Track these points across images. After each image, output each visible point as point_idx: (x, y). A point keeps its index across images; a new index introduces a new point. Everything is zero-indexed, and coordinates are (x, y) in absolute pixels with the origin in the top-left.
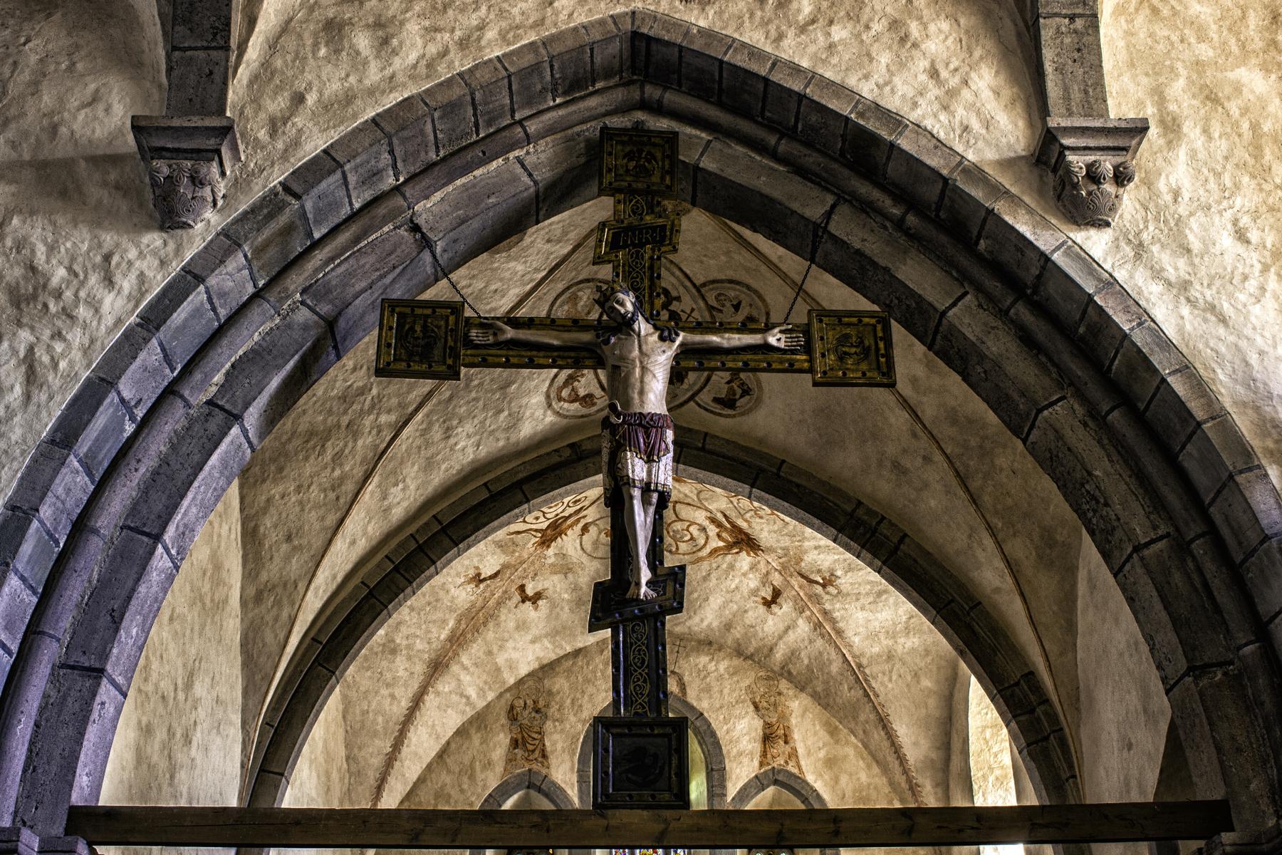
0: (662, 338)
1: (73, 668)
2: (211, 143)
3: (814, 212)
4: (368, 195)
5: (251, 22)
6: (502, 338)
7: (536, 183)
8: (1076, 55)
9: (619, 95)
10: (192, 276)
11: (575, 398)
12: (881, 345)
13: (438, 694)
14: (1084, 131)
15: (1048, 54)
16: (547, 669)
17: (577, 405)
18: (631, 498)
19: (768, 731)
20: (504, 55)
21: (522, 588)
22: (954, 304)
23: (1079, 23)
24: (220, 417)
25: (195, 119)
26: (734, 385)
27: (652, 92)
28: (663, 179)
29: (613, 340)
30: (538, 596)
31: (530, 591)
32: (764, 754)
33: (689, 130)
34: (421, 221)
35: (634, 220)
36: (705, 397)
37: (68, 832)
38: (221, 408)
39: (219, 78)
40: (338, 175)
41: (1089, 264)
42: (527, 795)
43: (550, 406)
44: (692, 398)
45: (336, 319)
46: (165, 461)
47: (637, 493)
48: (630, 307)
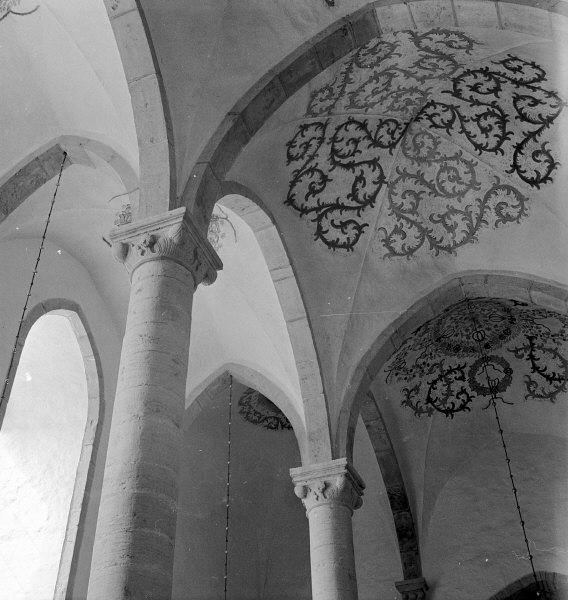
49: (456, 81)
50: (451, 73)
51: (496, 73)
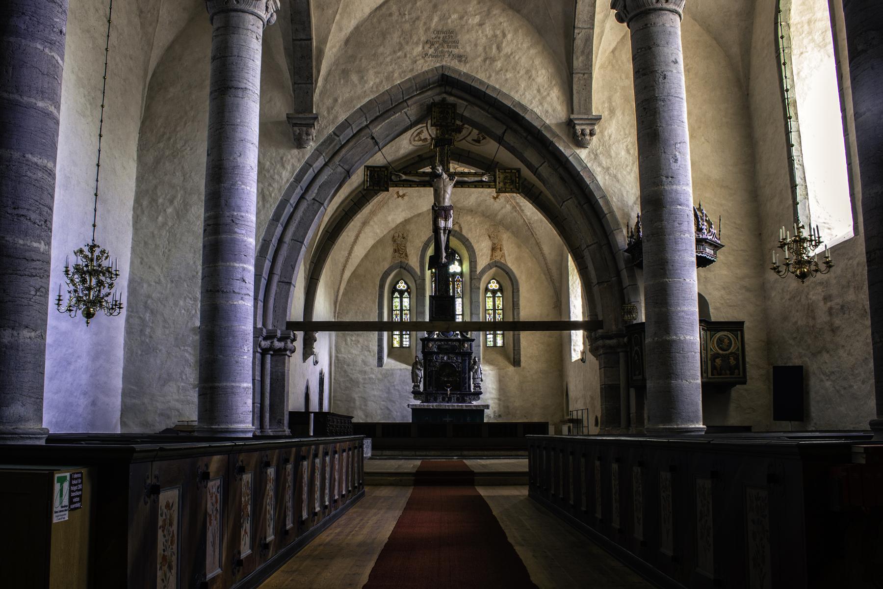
0: (450, 180)
1: (282, 282)
2: (312, 122)
3: (499, 132)
4: (358, 129)
5: (319, 72)
7: (411, 121)
8: (584, 88)
9: (437, 90)
10: (308, 165)
11: (420, 140)
12: (517, 179)
13: (365, 233)
14: (581, 119)
15: (575, 87)
16: (407, 221)
17: (421, 142)
18: (440, 233)
20: (401, 83)
21: (398, 193)
23: (586, 76)
24: (317, 204)
25: (306, 114)
26: (480, 135)
27: (448, 89)
28: (451, 121)
30: (404, 195)
31: (401, 193)
32: (492, 255)
33: (460, 101)
34: (374, 136)
36: (469, 139)
38: (317, 201)
39: (309, 94)
40: (350, 128)
41: (580, 160)
42: (400, 271)
43: (411, 143)
44: (464, 139)
45: (350, 170)
46: (302, 218)
47: (442, 231)
48: (440, 171)
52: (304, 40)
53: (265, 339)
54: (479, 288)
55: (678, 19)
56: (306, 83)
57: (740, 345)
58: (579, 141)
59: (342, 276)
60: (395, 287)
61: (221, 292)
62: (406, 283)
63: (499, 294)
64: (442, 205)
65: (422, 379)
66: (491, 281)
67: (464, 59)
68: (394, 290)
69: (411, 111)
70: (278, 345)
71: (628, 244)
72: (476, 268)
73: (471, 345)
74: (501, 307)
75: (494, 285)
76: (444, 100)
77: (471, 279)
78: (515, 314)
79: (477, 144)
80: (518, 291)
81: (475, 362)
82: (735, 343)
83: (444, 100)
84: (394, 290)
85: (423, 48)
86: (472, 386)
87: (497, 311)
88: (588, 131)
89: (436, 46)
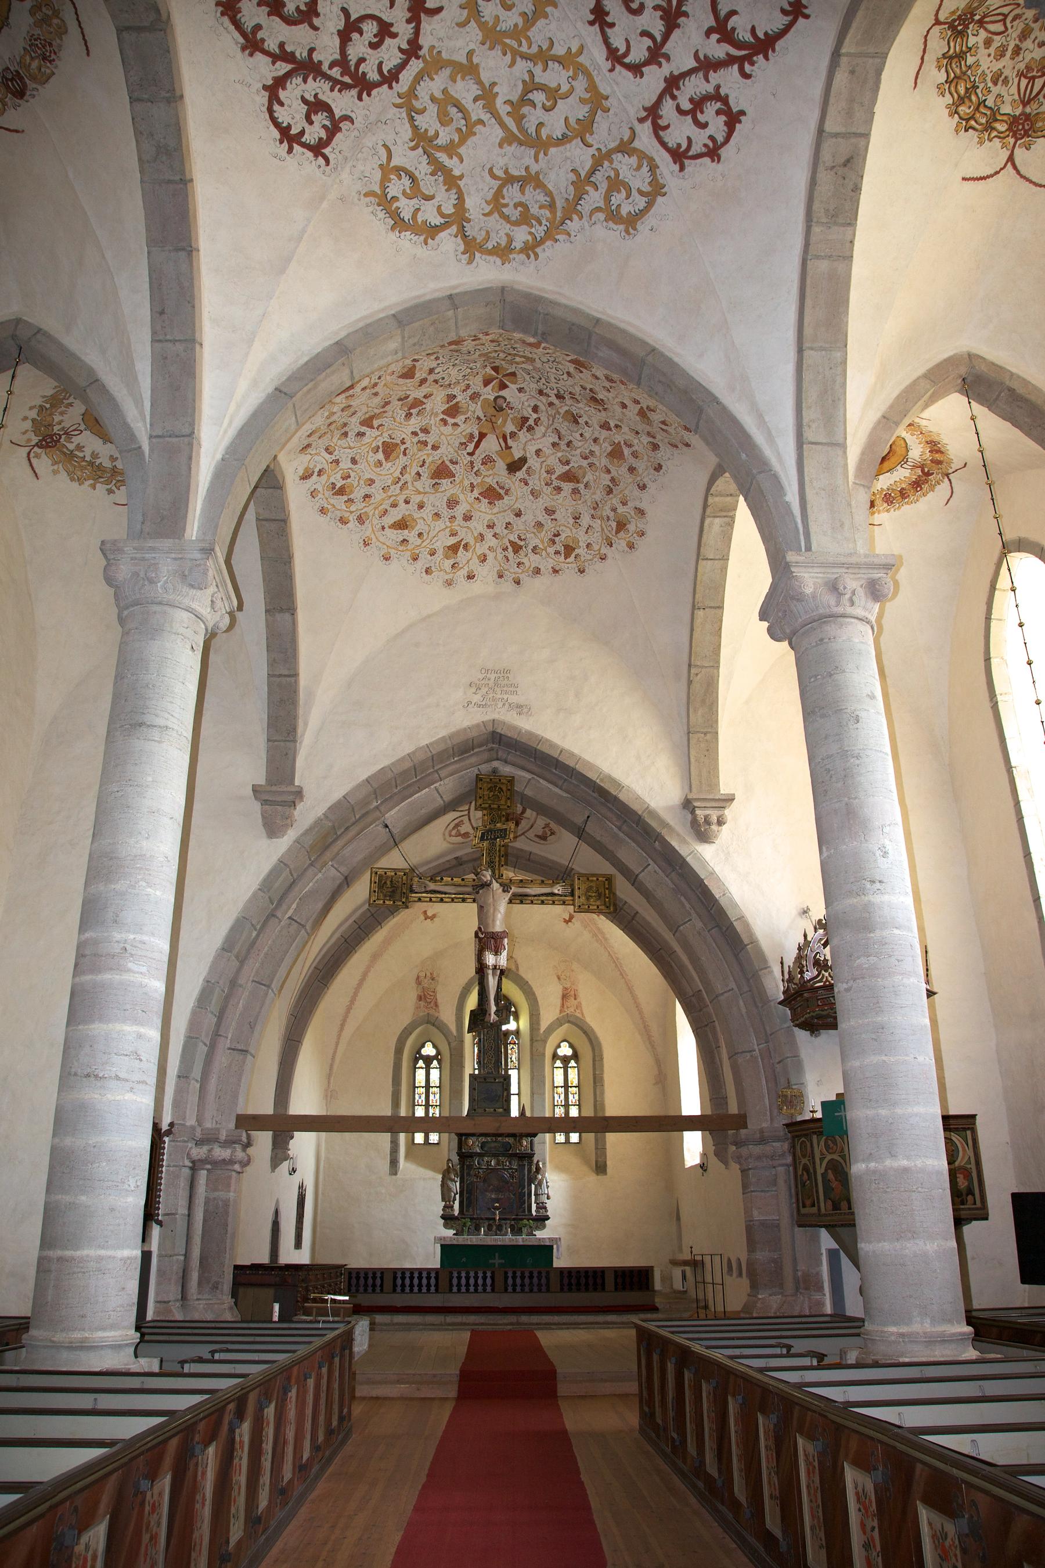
0: (504, 891)
1: (233, 1049)
4: (363, 811)
5: (306, 724)
6: (428, 889)
8: (706, 753)
11: (459, 835)
12: (607, 891)
18: (488, 974)
19: (565, 992)
21: (425, 912)
22: (643, 871)
23: (708, 736)
26: (547, 830)
28: (506, 802)
29: (481, 891)
30: (434, 916)
31: (429, 914)
35: (492, 827)
36: (531, 834)
37: (237, 1127)
38: (296, 921)
43: (445, 839)
47: (490, 972)
48: (489, 878)
49: (413, 50)
50: (418, 78)
51: (345, 86)
52: (285, 676)
53: (199, 1143)
54: (544, 1055)
55: (870, 632)
56: (285, 741)
57: (970, 1152)
58: (703, 835)
59: (339, 1036)
60: (419, 1052)
61: (92, 1079)
62: (434, 1046)
63: (573, 1063)
64: (491, 930)
65: (457, 1196)
66: (562, 1044)
67: (525, 710)
68: (417, 1056)
69: (447, 787)
70: (221, 1153)
71: (784, 993)
72: (538, 1024)
73: (532, 1143)
74: (575, 1083)
75: (565, 1050)
76: (495, 771)
77: (532, 1040)
78: (598, 1093)
79: (542, 842)
80: (602, 1059)
81: (538, 1169)
82: (964, 1150)
83: (495, 771)
84: (417, 1056)
85: (465, 693)
86: (534, 1206)
87: (570, 1089)
88: (714, 819)
89: (484, 690)
